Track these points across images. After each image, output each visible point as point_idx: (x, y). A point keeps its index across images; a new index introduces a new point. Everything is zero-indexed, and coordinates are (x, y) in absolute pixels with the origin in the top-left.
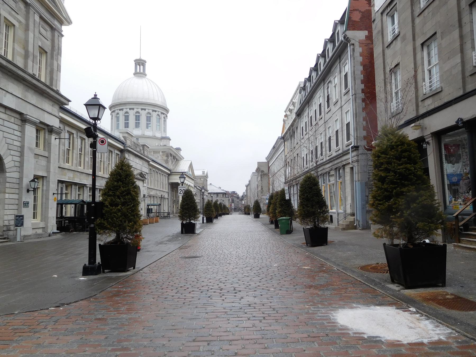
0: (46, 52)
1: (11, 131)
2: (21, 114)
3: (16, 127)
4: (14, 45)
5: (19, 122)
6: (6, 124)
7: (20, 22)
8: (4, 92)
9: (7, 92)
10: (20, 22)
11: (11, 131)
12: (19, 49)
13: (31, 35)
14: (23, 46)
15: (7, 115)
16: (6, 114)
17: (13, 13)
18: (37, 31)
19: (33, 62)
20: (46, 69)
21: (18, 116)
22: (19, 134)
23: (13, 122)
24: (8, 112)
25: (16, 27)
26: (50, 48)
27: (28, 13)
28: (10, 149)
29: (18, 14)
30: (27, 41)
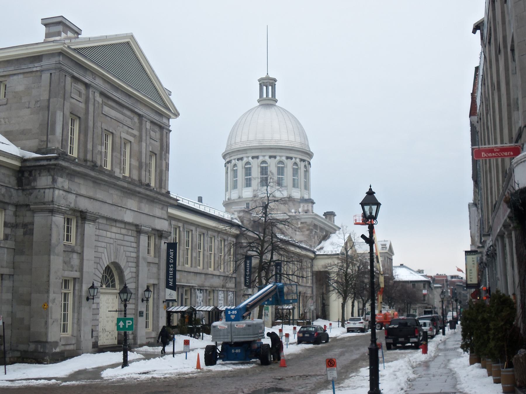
0: (156, 154)
1: (128, 244)
2: (137, 226)
3: (132, 239)
4: (130, 161)
5: (135, 234)
6: (127, 238)
7: (134, 136)
8: (125, 209)
9: (127, 209)
10: (134, 136)
11: (128, 244)
12: (135, 163)
13: (144, 144)
14: (137, 158)
15: (126, 230)
16: (125, 228)
17: (130, 130)
18: (148, 138)
19: (146, 171)
20: (156, 171)
21: (133, 228)
22: (134, 245)
23: (130, 235)
24: (127, 227)
25: (132, 143)
26: (159, 149)
27: (141, 123)
28: (128, 262)
29: (133, 129)
30: (140, 152)
